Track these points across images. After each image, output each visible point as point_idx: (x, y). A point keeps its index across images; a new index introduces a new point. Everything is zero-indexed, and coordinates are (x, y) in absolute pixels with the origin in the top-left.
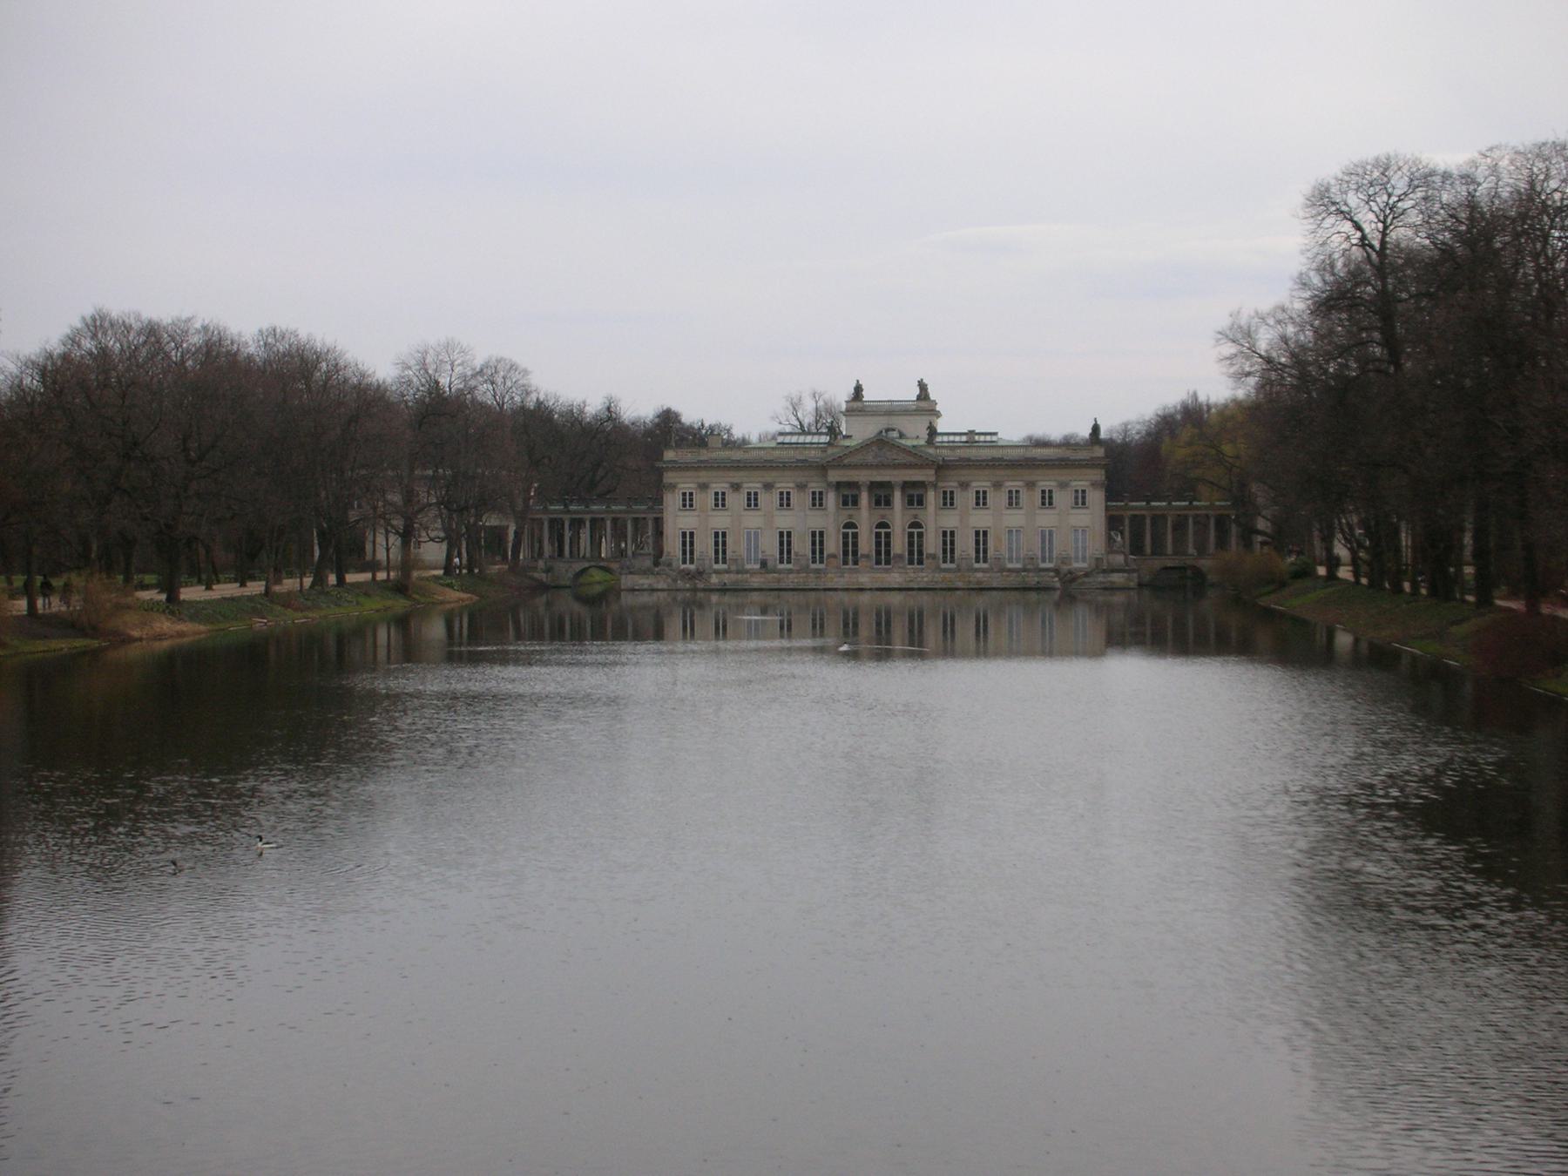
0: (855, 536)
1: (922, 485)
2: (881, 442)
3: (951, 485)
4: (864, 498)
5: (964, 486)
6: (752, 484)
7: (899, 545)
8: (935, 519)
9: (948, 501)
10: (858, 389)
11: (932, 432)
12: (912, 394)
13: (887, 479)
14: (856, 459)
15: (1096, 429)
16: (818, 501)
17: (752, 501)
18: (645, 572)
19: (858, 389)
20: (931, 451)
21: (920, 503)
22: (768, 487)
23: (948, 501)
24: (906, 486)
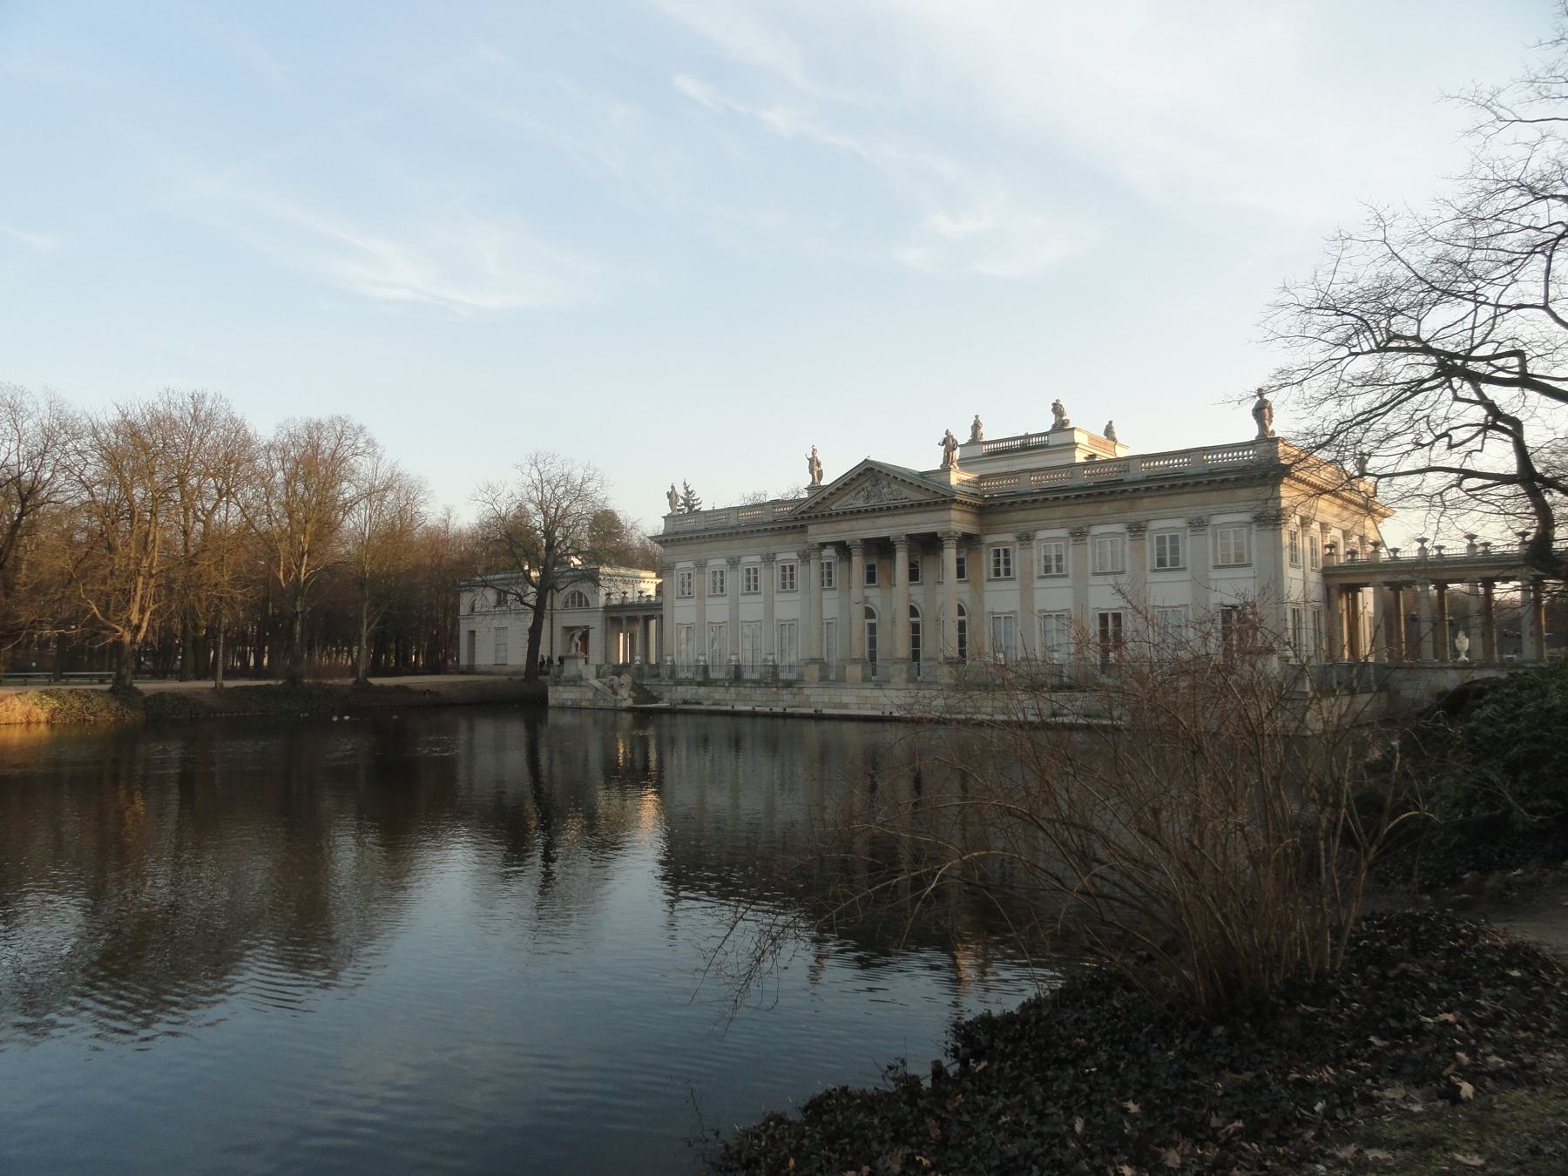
5: (1026, 538)
10: (976, 426)
12: (1046, 422)
13: (884, 533)
19: (976, 426)
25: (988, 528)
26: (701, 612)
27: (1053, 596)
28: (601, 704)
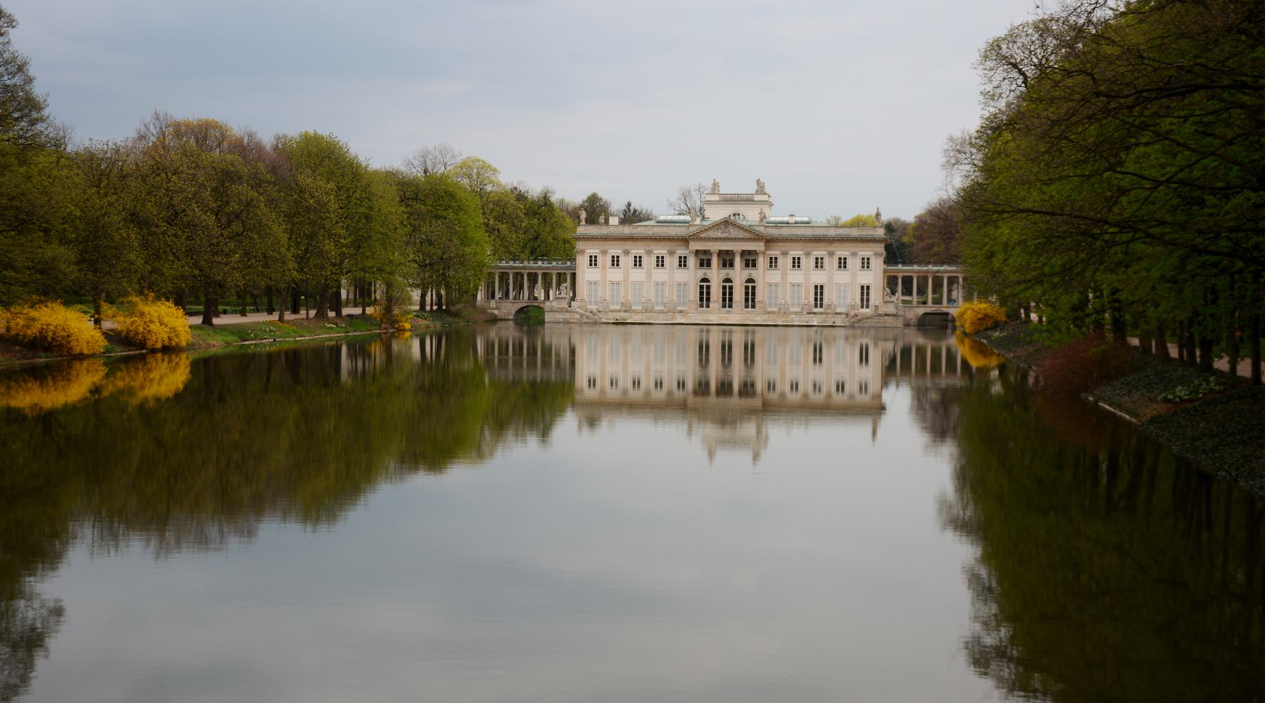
0: (708, 287)
1: (754, 253)
2: (726, 223)
3: (774, 253)
4: (715, 261)
5: (785, 254)
6: (638, 250)
7: (739, 295)
8: (763, 275)
9: (773, 262)
10: (716, 185)
11: (763, 218)
14: (712, 234)
15: (878, 215)
16: (683, 262)
17: (638, 262)
18: (561, 310)
20: (762, 229)
21: (754, 265)
22: (649, 253)
23: (773, 262)
24: (743, 253)
25: (767, 248)
26: (604, 276)
27: (796, 276)
28: (585, 320)
